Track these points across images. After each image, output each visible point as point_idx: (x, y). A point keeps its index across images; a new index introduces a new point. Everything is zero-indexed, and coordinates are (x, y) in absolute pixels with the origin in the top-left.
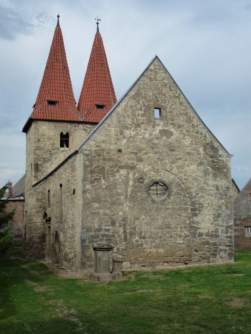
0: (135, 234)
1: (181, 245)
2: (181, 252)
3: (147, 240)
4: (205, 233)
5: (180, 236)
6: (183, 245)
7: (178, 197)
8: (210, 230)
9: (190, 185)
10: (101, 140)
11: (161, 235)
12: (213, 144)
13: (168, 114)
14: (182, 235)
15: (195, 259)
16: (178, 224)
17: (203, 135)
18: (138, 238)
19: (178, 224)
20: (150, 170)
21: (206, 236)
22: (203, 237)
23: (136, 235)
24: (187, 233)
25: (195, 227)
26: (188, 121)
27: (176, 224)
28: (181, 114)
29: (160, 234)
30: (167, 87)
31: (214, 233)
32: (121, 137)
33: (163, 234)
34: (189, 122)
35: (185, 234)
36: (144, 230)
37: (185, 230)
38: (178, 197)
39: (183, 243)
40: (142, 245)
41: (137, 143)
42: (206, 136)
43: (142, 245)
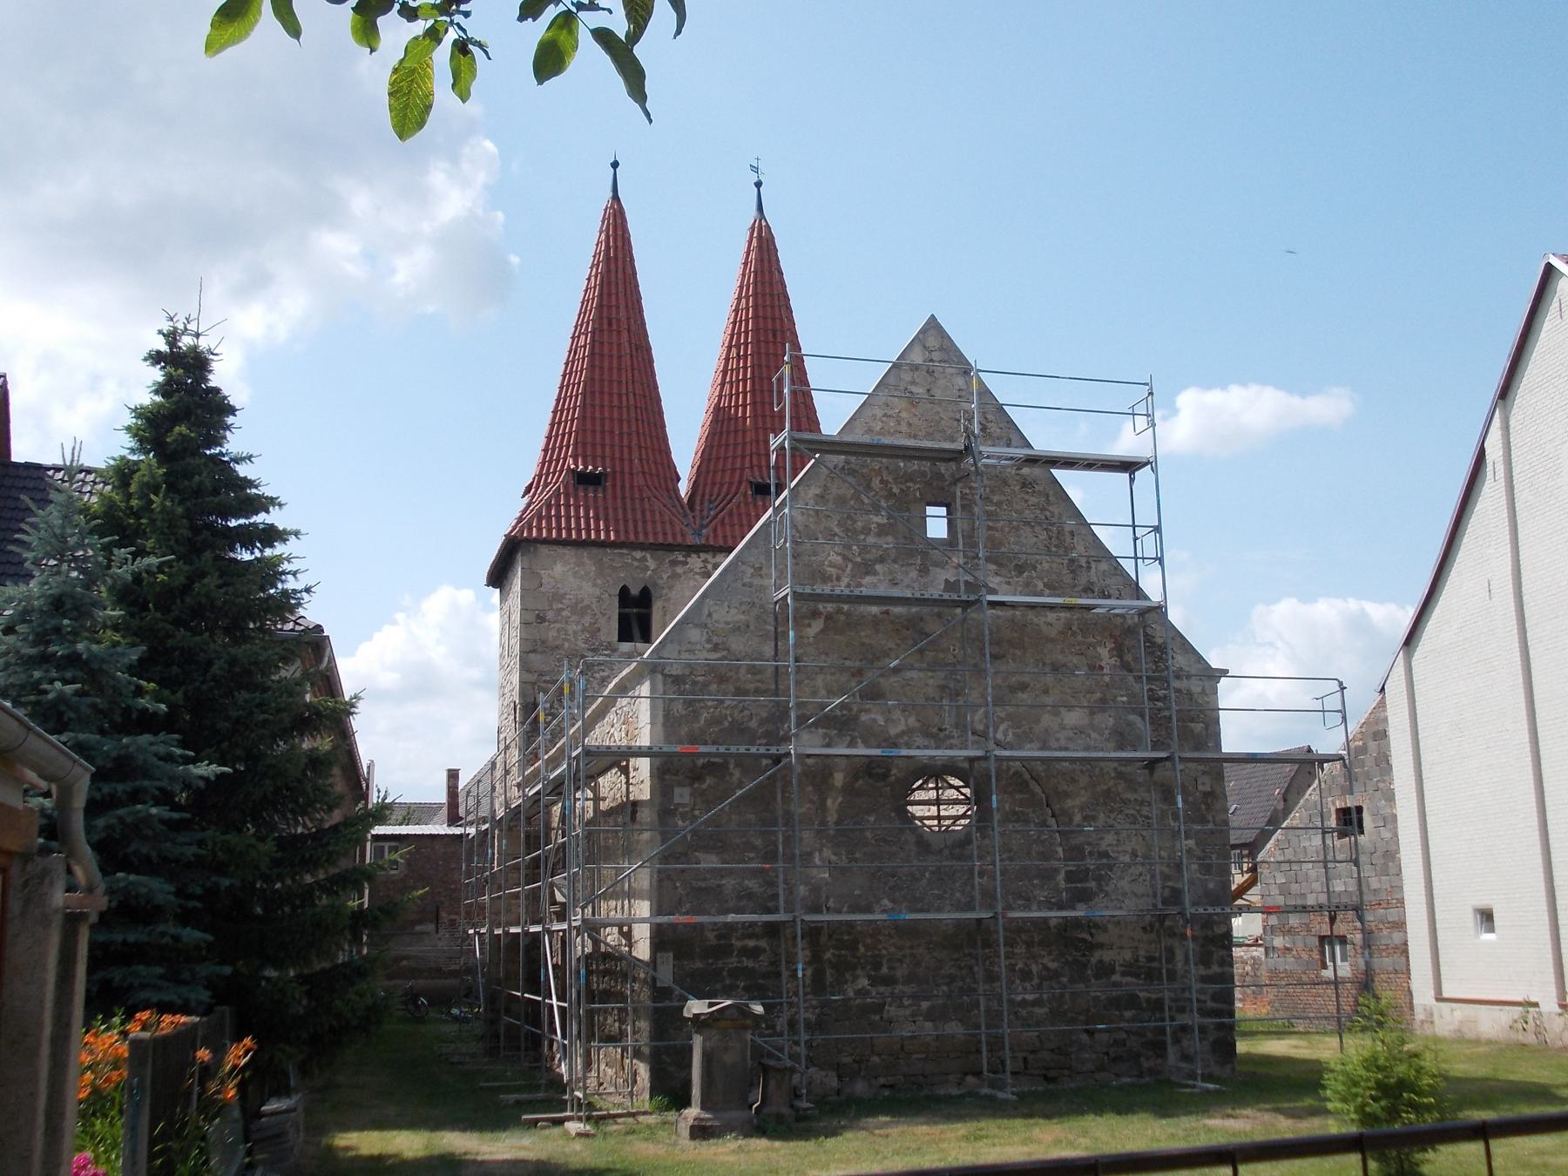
1: (1029, 1009)
3: (899, 988)
4: (1121, 965)
5: (1026, 975)
8: (1142, 953)
9: (1064, 787)
10: (728, 623)
11: (953, 971)
12: (1149, 631)
14: (1034, 971)
21: (1124, 974)
22: (1116, 978)
24: (1053, 965)
25: (1084, 940)
26: (1054, 549)
35: (1046, 968)
39: (1035, 1003)
40: (879, 1008)
43: (879, 1008)
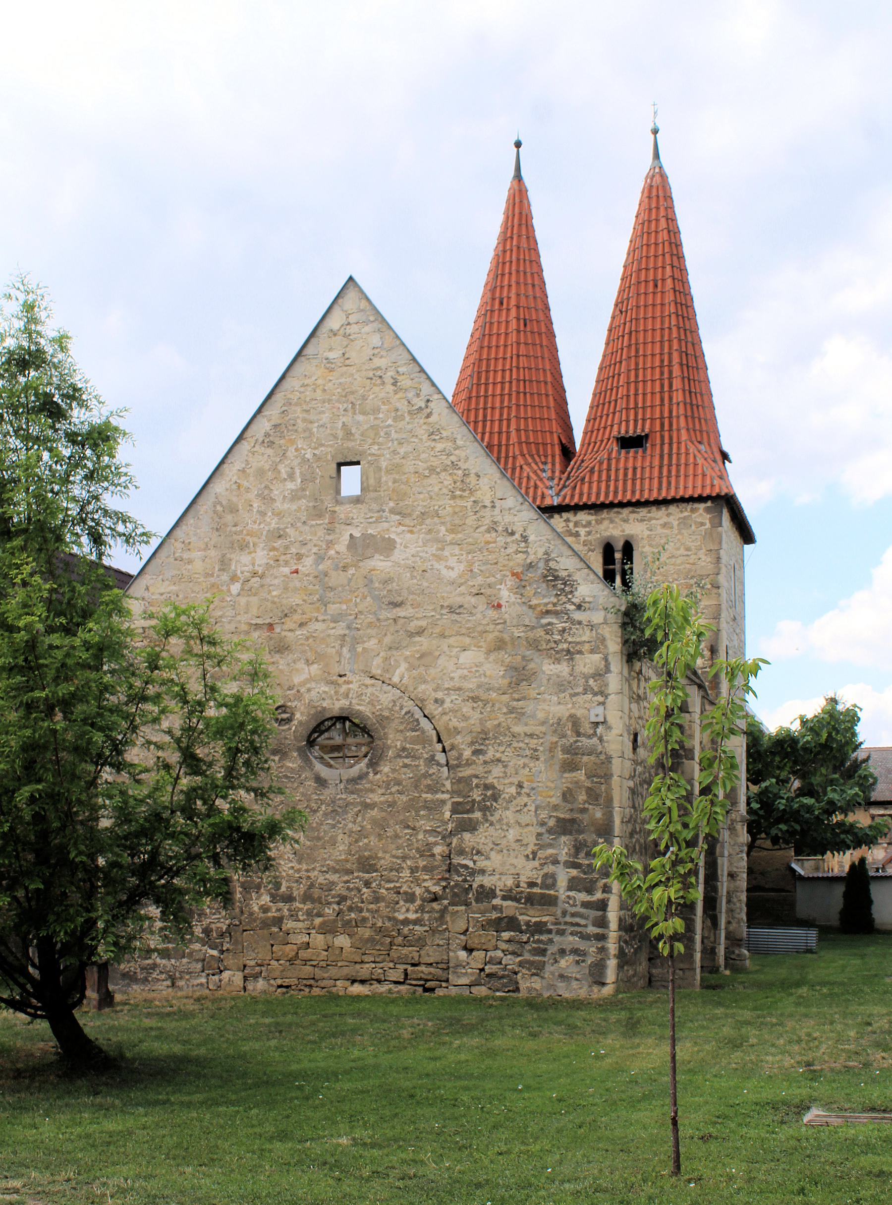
0: (258, 887)
1: (411, 927)
2: (410, 948)
3: (297, 904)
4: (501, 890)
5: (410, 898)
6: (417, 928)
7: (406, 766)
8: (523, 879)
9: (454, 723)
10: (162, 594)
11: (345, 893)
12: (552, 564)
13: (384, 479)
14: (417, 893)
15: (459, 977)
16: (404, 858)
17: (517, 536)
18: (268, 898)
19: (404, 858)
20: (311, 679)
21: (504, 898)
22: (496, 901)
23: (262, 890)
24: (436, 889)
25: (466, 867)
26: (458, 493)
27: (397, 858)
28: (432, 470)
29: (340, 889)
30: (383, 383)
31: (536, 890)
32: (225, 577)
33: (348, 888)
34: (461, 496)
35: (427, 890)
36: (288, 875)
37: (427, 877)
38: (406, 766)
39: (416, 922)
40: (279, 921)
41: (274, 593)
42: (525, 539)
43: (279, 921)
